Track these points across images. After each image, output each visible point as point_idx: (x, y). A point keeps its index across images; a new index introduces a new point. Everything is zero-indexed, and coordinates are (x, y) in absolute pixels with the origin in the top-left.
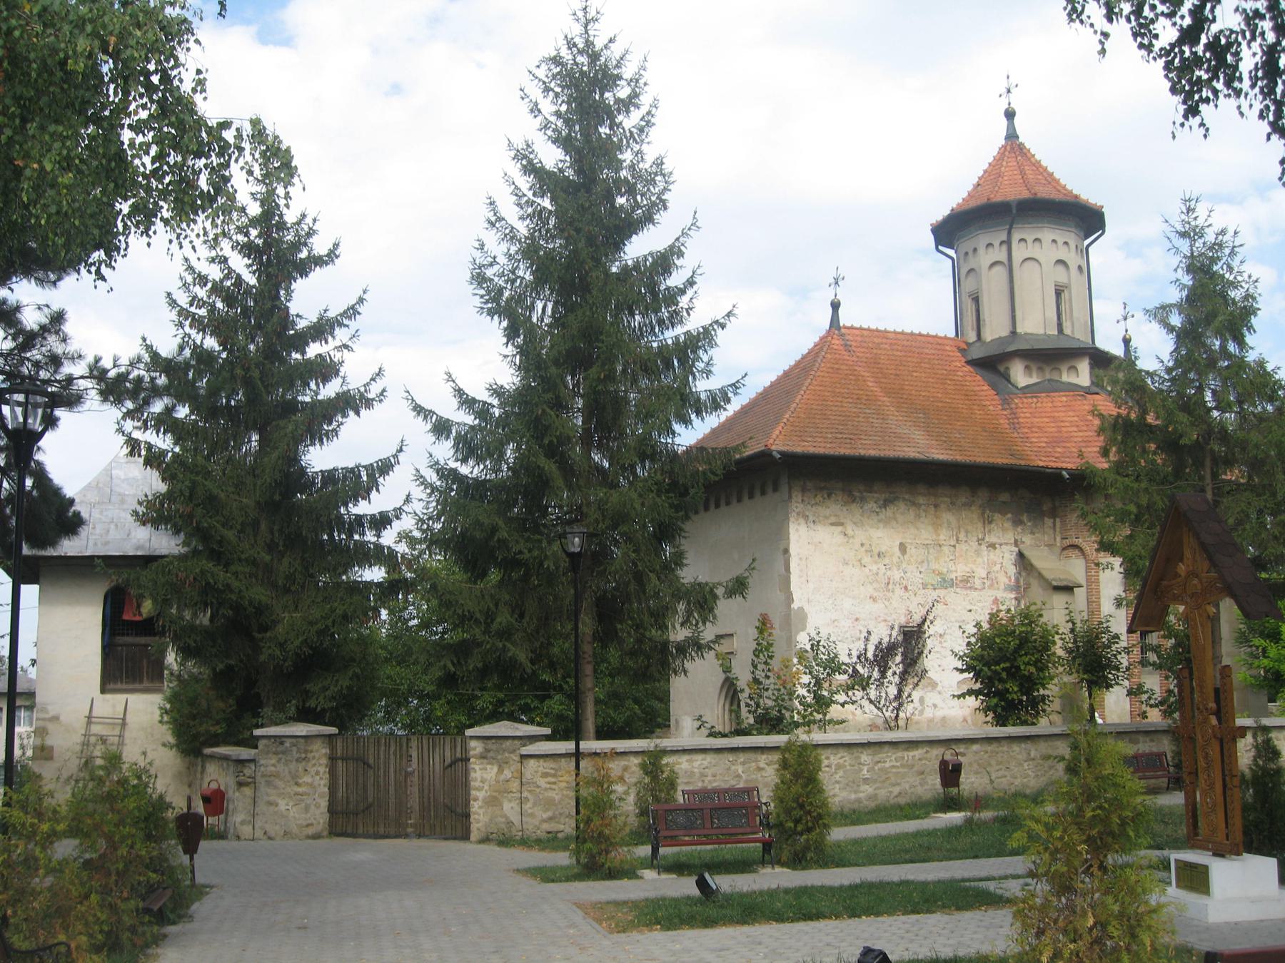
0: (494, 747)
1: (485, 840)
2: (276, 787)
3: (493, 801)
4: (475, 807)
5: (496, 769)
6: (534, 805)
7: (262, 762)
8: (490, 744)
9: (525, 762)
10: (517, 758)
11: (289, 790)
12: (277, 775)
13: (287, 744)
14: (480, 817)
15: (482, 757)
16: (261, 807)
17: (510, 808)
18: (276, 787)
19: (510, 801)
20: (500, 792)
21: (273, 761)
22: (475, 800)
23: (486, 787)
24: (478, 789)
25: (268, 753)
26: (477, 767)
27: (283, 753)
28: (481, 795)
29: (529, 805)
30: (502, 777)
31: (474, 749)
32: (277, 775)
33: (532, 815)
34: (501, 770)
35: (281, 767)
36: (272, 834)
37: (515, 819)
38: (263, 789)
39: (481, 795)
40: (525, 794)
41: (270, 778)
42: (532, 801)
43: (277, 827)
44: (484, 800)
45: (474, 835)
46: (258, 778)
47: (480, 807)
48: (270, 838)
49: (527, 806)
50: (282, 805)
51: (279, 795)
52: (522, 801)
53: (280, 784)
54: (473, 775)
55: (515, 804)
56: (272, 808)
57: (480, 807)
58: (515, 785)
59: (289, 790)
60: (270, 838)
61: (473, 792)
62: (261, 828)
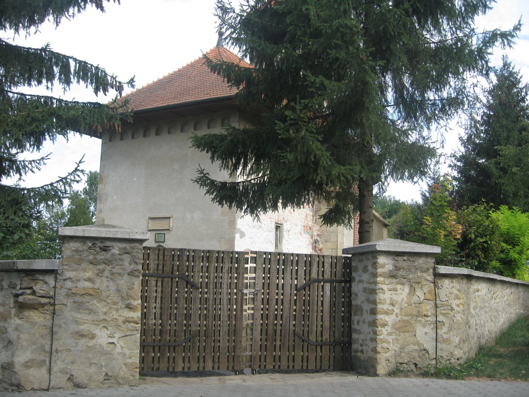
0: (405, 265)
1: (394, 373)
2: (91, 311)
3: (404, 327)
4: (384, 333)
5: (407, 289)
6: (450, 329)
7: (68, 274)
8: (401, 262)
9: (440, 282)
10: (431, 278)
11: (115, 314)
12: (96, 294)
13: (116, 251)
14: (388, 344)
15: (392, 276)
16: (64, 340)
17: (423, 334)
18: (91, 311)
19: (424, 326)
20: (411, 315)
21: (88, 274)
22: (384, 325)
23: (397, 311)
24: (387, 313)
25: (80, 261)
26: (385, 287)
27: (107, 262)
28: (390, 319)
29: (444, 329)
30: (415, 299)
31: (383, 266)
32: (96, 294)
33: (445, 341)
34: (412, 290)
35: (102, 283)
36: (82, 378)
37: (430, 346)
38: (68, 313)
39: (390, 319)
40: (440, 318)
41: (81, 300)
42: (447, 325)
43: (93, 369)
44: (393, 326)
45: (382, 368)
46: (61, 298)
47: (390, 334)
48: (78, 386)
49: (442, 331)
50: (102, 337)
51: (104, 323)
52: (437, 325)
53: (100, 307)
54: (380, 296)
55: (430, 330)
56: (82, 342)
57: (390, 334)
58: (428, 308)
59: (115, 314)
60: (78, 386)
61: (380, 317)
62: (63, 371)
